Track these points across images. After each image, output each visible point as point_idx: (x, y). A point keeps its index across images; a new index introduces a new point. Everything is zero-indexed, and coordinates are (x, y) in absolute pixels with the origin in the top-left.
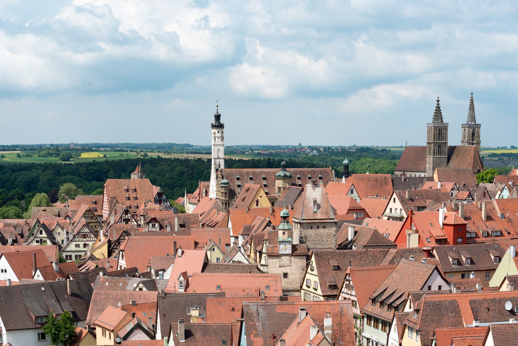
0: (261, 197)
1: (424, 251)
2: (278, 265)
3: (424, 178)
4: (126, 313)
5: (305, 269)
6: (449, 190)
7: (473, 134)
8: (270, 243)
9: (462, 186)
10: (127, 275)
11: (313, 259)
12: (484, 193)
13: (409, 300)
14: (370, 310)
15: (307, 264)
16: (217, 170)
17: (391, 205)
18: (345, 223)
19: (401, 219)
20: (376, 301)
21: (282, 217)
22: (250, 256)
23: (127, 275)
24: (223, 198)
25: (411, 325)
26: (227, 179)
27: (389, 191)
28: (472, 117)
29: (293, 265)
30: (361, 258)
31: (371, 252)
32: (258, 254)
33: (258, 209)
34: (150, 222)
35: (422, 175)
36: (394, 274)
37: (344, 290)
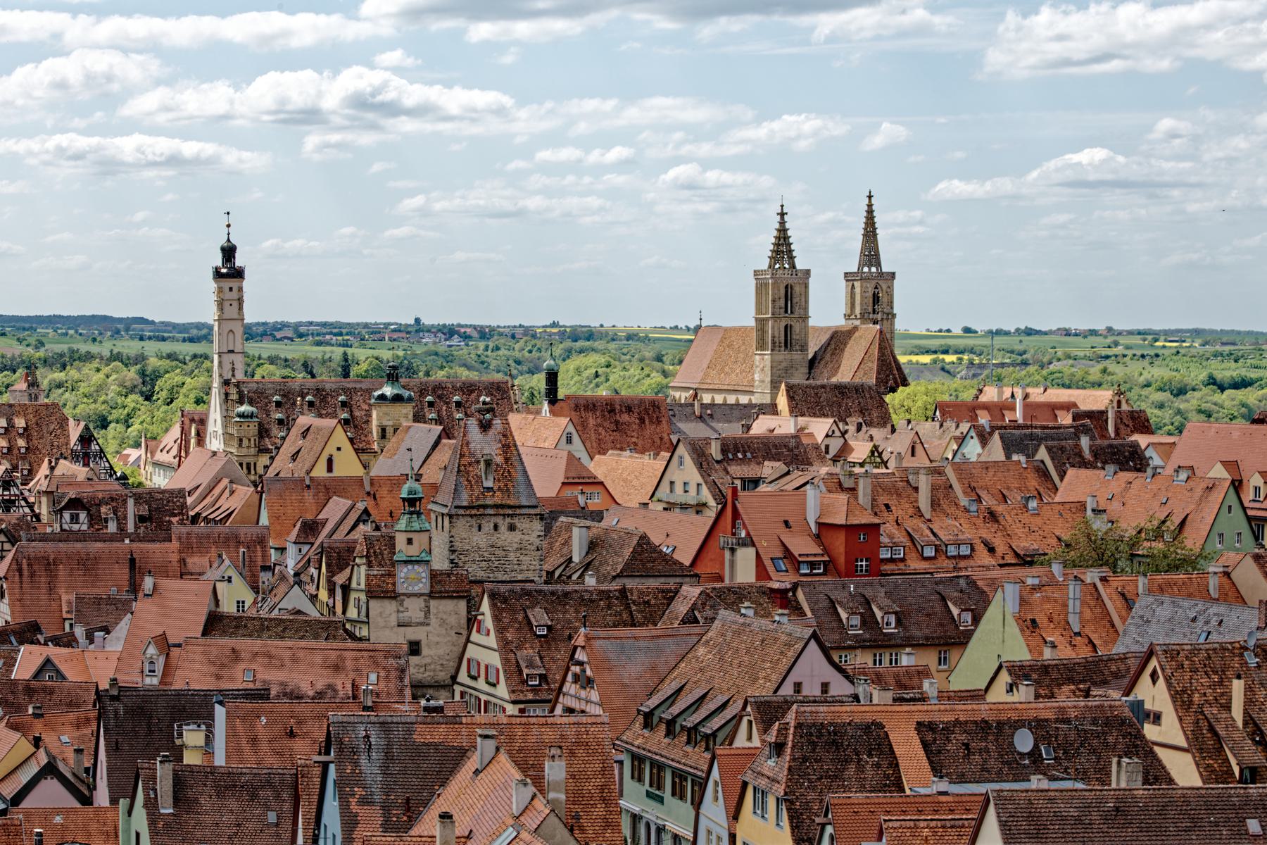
0: (339, 449)
1: (772, 590)
2: (393, 620)
3: (750, 406)
4: (18, 735)
5: (465, 632)
6: (820, 438)
7: (876, 299)
8: (370, 565)
9: (852, 428)
10: (13, 639)
11: (486, 606)
12: (913, 448)
13: (745, 720)
14: (636, 743)
15: (469, 620)
16: (226, 383)
17: (675, 474)
18: (563, 519)
19: (700, 507)
20: (655, 720)
21: (404, 500)
22: (317, 596)
23: (13, 639)
24: (244, 451)
25: (763, 783)
26: (251, 404)
27: (661, 439)
28: (871, 253)
29: (433, 621)
30: (609, 606)
31: (635, 593)
32: (339, 592)
33: (334, 479)
34: (66, 508)
35: (744, 400)
36: (701, 651)
37: (570, 687)
